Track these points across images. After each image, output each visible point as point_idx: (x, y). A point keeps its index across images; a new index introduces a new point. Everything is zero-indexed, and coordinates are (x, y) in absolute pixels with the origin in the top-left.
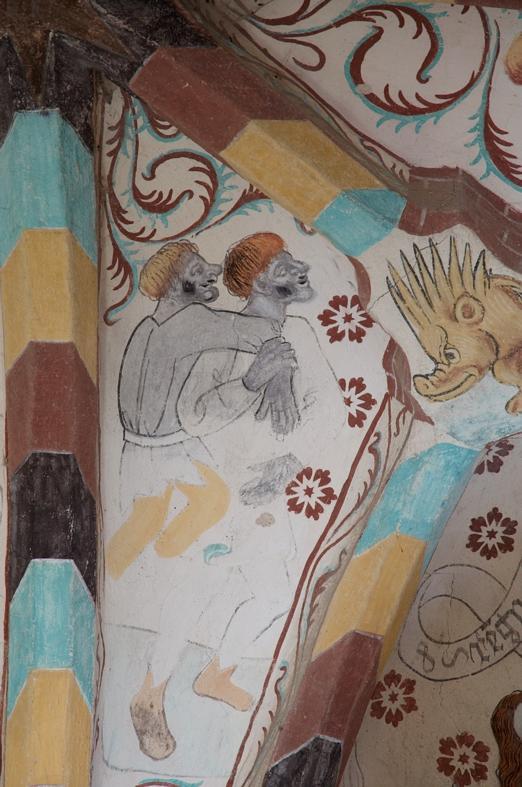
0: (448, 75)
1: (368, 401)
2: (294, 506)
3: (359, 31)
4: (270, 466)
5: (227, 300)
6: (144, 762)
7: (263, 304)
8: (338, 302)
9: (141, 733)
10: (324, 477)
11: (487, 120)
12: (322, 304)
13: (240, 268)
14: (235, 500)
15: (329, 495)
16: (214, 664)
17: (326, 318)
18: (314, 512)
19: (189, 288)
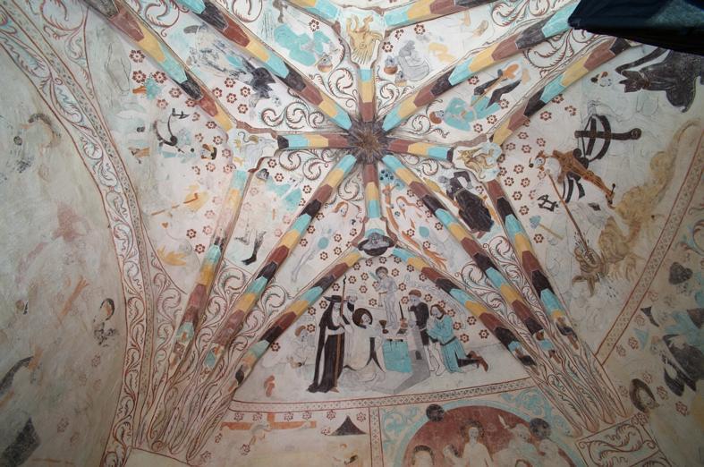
0: (340, 73)
1: (398, 32)
2: (424, 31)
3: (345, 91)
4: (421, 40)
5: (399, 69)
6: (490, 26)
7: (396, 63)
8: (386, 51)
9: (484, 30)
10: (415, 29)
11: (341, 61)
12: (389, 53)
13: (393, 71)
14: (431, 42)
15: (418, 26)
16: (463, 24)
17: (390, 51)
18: (422, 27)
19: (402, 77)
